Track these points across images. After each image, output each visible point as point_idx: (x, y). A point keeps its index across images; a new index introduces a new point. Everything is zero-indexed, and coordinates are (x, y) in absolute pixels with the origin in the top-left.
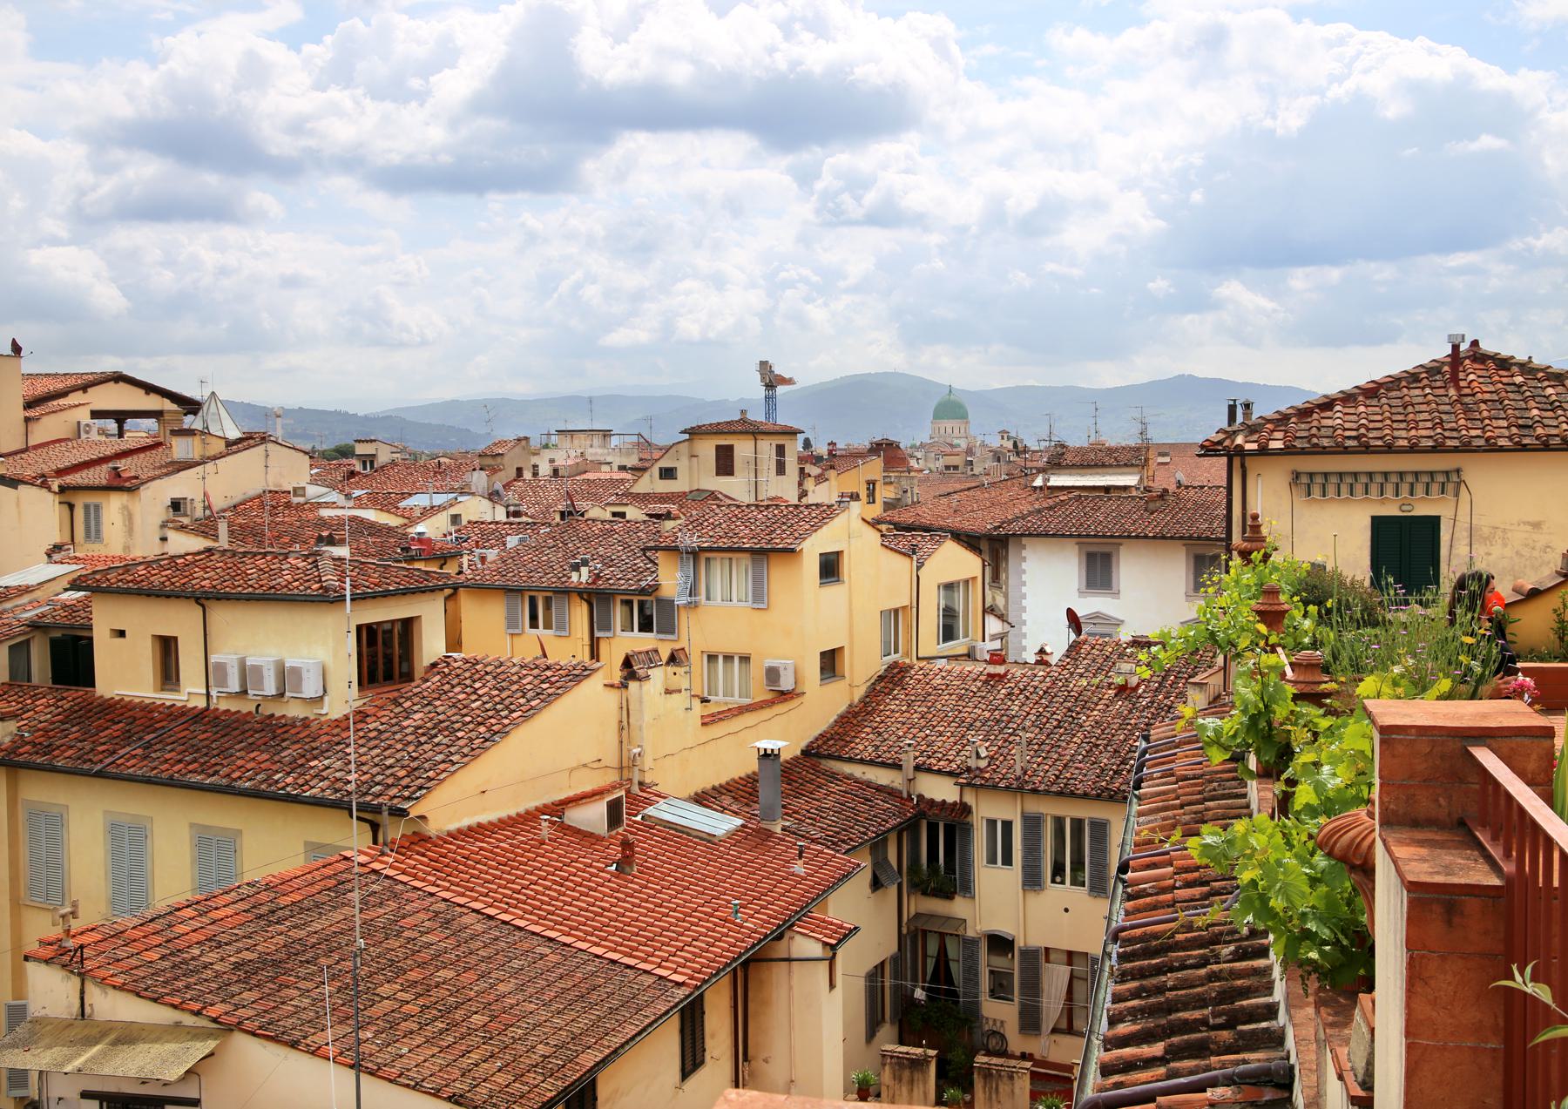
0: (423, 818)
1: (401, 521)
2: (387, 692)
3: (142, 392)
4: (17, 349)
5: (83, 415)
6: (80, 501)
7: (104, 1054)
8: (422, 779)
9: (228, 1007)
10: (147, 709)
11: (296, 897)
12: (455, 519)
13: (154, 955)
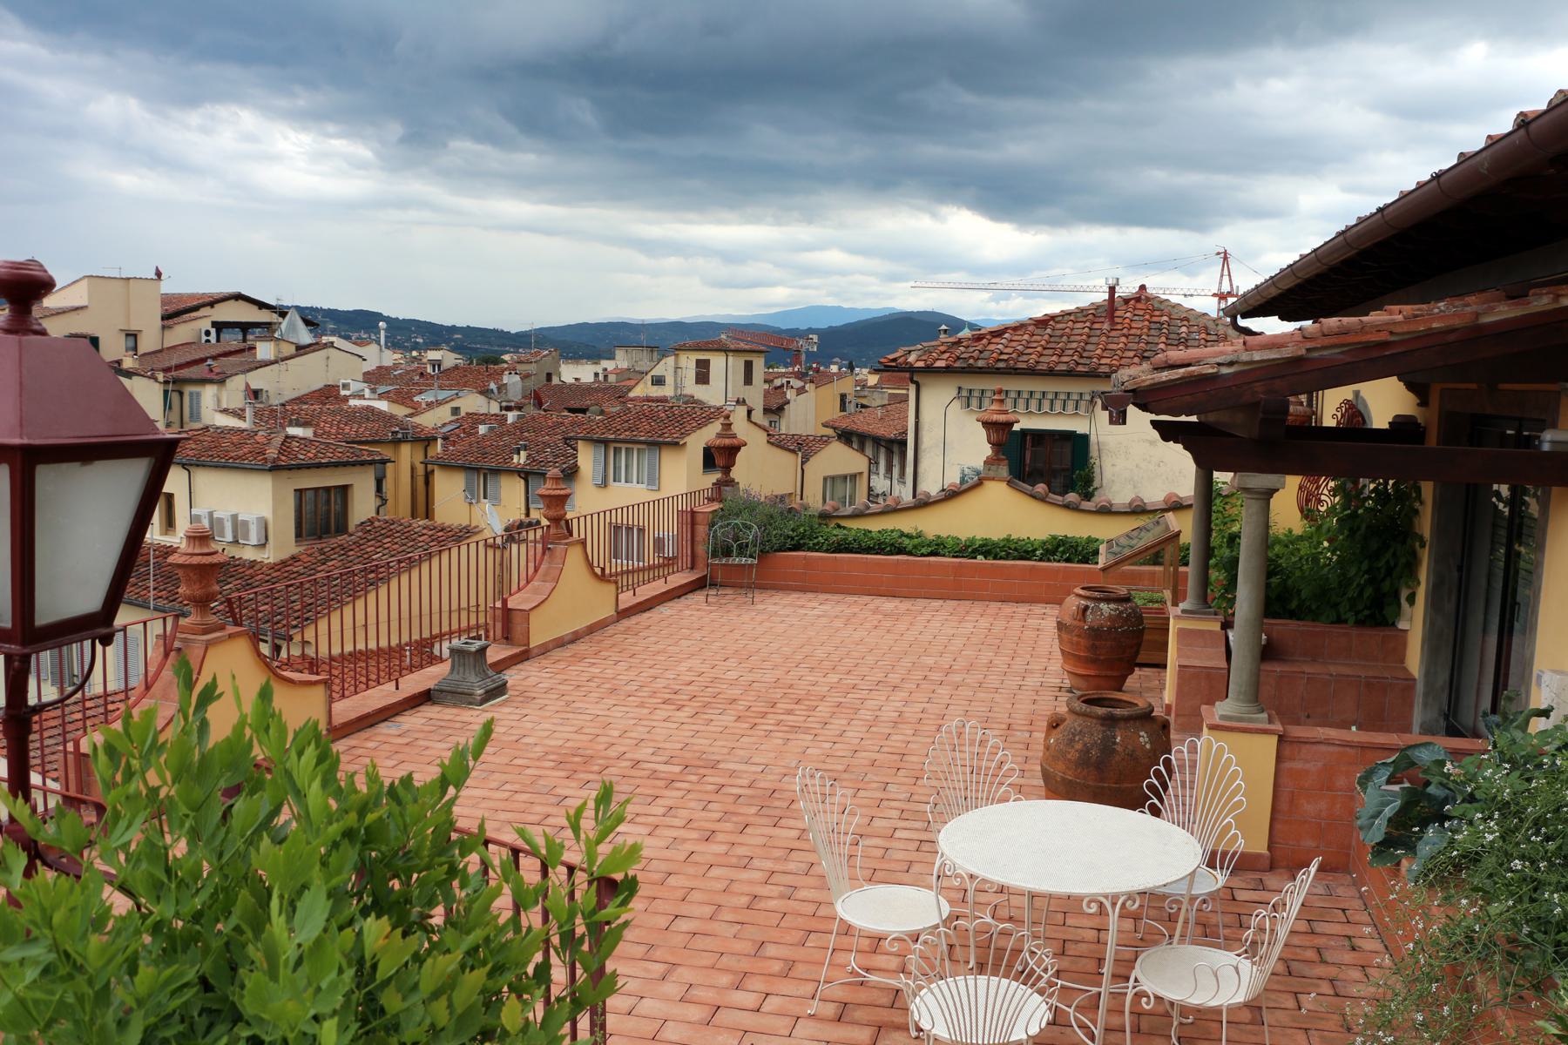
1: (410, 411)
3: (255, 308)
4: (159, 274)
6: (188, 389)
12: (456, 411)
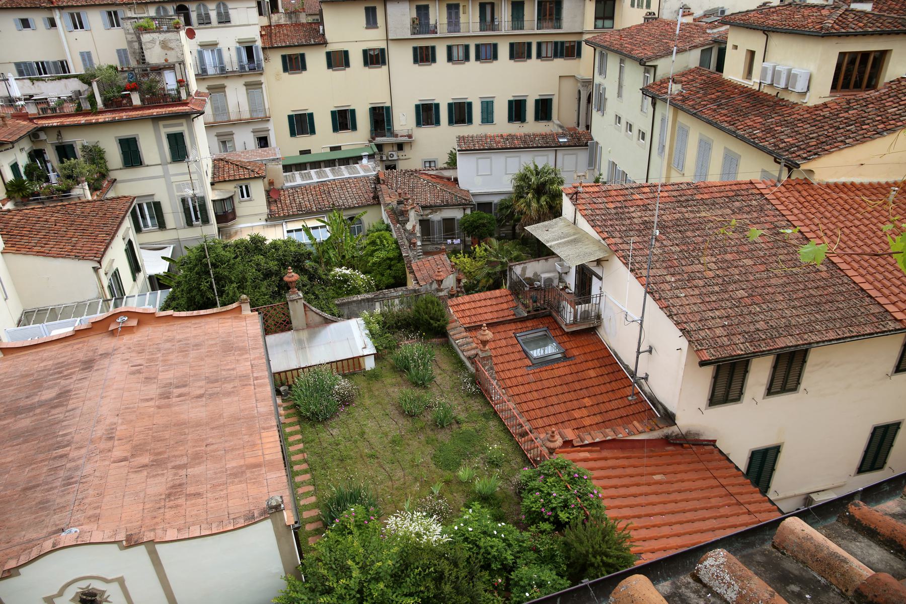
0: (811, 171)
2: (849, 95)
9: (621, 241)
11: (706, 196)
13: (612, 206)
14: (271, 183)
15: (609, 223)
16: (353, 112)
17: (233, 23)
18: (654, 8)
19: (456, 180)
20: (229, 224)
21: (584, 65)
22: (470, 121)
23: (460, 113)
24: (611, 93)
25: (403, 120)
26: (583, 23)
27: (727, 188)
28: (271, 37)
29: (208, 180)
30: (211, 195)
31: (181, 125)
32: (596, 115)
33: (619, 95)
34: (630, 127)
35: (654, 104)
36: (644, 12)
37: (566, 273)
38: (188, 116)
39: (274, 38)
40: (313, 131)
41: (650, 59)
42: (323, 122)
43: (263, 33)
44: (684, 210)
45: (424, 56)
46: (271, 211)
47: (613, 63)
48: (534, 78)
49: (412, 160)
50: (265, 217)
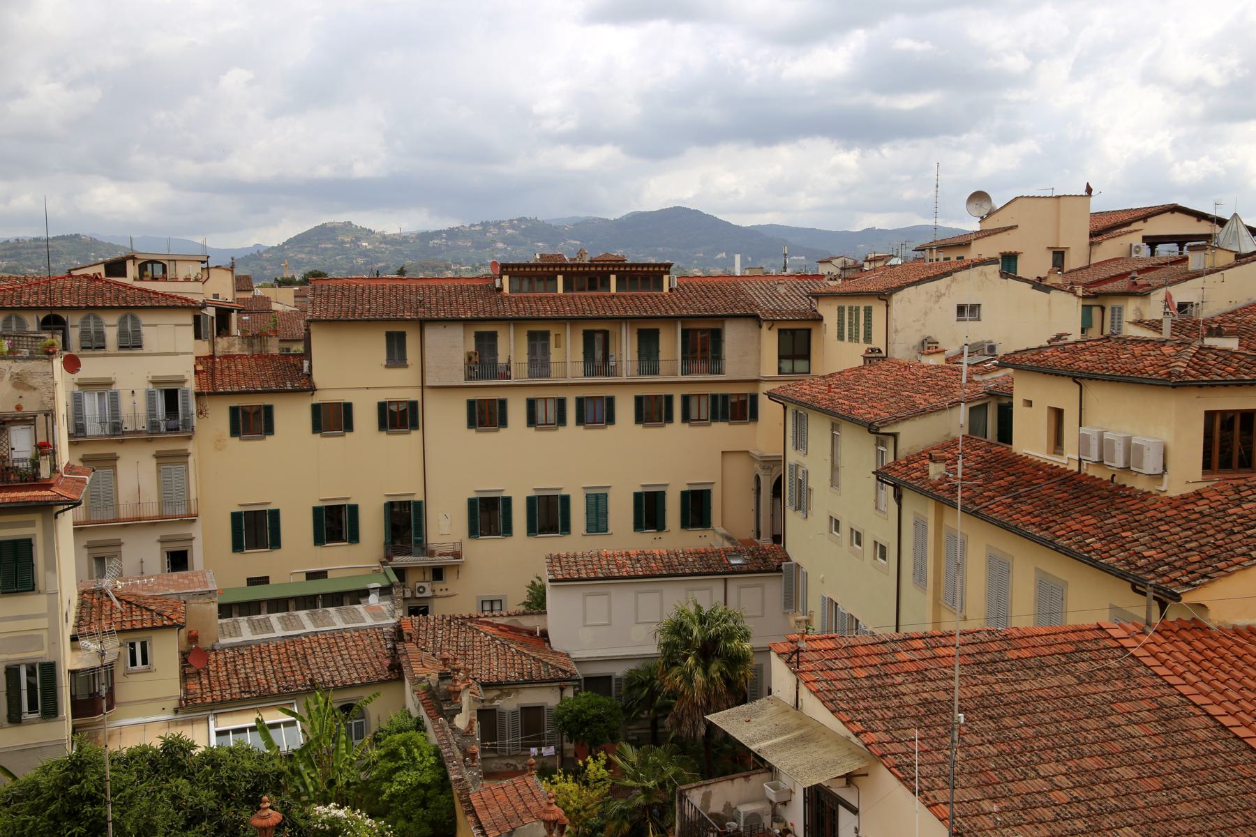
0: (1202, 607)
2: (1236, 478)
3: (1195, 219)
4: (1089, 190)
5: (1136, 240)
6: (1110, 304)
7: (785, 744)
8: (1212, 566)
9: (887, 737)
10: (1038, 466)
11: (1026, 653)
13: (862, 673)
14: (193, 638)
15: (862, 704)
16: (354, 510)
17: (146, 350)
18: (878, 341)
19: (545, 634)
20: (98, 718)
21: (767, 432)
22: (566, 529)
23: (549, 514)
24: (818, 480)
25: (446, 525)
26: (758, 364)
27: (1061, 638)
28: (212, 375)
29: (68, 630)
30: (70, 661)
31: (32, 524)
32: (793, 520)
33: (834, 482)
34: (858, 538)
35: (898, 498)
36: (862, 347)
37: (785, 803)
38: (48, 509)
39: (218, 376)
40: (276, 543)
41: (885, 423)
42: (297, 528)
43: (200, 368)
44: (991, 678)
45: (486, 416)
46: (187, 692)
47: (818, 430)
48: (678, 455)
49: (459, 598)
50: (175, 704)
